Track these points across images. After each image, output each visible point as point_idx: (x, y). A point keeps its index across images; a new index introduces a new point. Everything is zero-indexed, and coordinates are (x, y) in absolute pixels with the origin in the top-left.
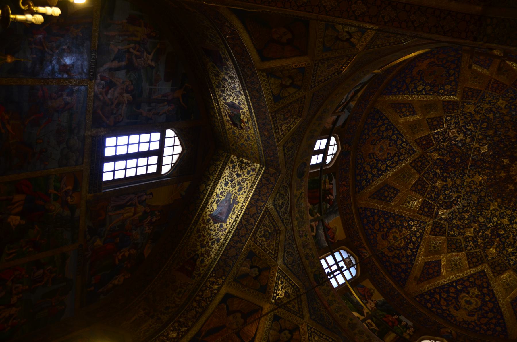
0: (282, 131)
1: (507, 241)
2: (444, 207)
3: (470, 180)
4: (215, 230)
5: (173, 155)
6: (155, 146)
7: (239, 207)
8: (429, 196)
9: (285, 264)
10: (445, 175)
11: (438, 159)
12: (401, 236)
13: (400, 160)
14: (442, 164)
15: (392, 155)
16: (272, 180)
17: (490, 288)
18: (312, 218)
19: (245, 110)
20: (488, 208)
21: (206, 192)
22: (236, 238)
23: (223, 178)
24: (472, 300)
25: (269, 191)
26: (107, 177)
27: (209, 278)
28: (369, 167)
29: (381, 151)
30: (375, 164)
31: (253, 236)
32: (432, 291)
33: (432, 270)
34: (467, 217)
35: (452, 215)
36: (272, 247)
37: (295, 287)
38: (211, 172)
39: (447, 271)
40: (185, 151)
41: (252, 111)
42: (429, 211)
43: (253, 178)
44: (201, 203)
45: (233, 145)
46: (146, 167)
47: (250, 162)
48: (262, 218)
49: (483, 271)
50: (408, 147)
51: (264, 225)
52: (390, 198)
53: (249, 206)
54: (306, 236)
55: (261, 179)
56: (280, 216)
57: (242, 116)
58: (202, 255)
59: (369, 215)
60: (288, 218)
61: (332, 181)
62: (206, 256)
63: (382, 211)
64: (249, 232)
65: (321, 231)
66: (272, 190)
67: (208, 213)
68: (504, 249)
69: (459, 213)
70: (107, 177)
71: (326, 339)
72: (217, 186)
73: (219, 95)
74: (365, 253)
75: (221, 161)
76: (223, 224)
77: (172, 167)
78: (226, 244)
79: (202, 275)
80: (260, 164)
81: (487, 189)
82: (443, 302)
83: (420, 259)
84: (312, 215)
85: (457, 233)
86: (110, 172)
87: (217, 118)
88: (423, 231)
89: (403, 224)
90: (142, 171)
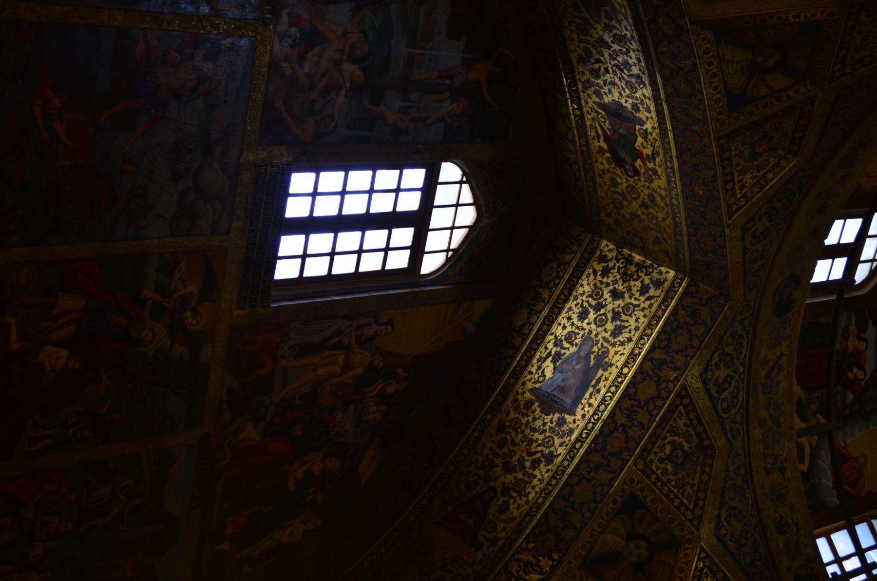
0: (742, 187)
4: (544, 431)
5: (452, 228)
6: (410, 202)
7: (612, 378)
9: (720, 538)
18: (803, 425)
19: (648, 126)
21: (530, 330)
23: (576, 298)
25: (695, 342)
26: (285, 270)
27: (517, 552)
31: (641, 456)
36: (688, 489)
38: (545, 279)
40: (485, 222)
41: (666, 130)
43: (655, 305)
44: (512, 358)
45: (609, 215)
46: (381, 252)
47: (649, 262)
51: (673, 432)
53: (638, 379)
54: (783, 470)
55: (675, 309)
56: (717, 412)
57: (640, 140)
58: (506, 491)
60: (739, 417)
61: (864, 331)
62: (514, 494)
64: (632, 444)
65: (825, 462)
66: (702, 341)
67: (530, 385)
70: (285, 270)
72: (560, 318)
73: (583, 83)
75: (575, 253)
76: (567, 417)
77: (448, 259)
78: (569, 471)
80: (677, 271)
84: (803, 418)
86: (296, 259)
87: (574, 141)
90: (371, 263)
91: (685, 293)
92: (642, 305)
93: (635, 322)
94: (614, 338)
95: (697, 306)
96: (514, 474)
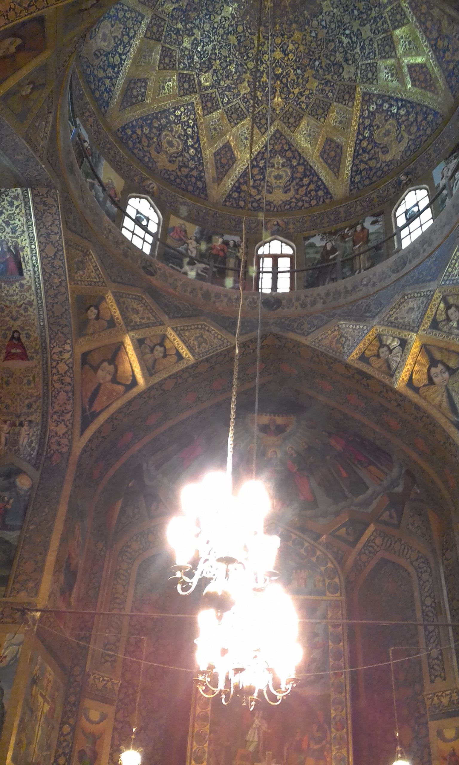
1: (289, 80)
2: (204, 70)
3: (220, 18)
4: (17, 294)
7: (29, 253)
8: (182, 66)
10: (189, 26)
11: (174, 9)
12: (174, 136)
13: (131, 38)
14: (180, 13)
15: (119, 37)
16: (50, 201)
17: (293, 149)
20: (252, 46)
22: (52, 292)
24: (281, 173)
28: (101, 71)
29: (105, 41)
30: (106, 62)
31: (70, 279)
32: (237, 185)
33: (225, 158)
34: (234, 70)
35: (217, 76)
36: (93, 275)
37: (137, 297)
39: (241, 152)
42: (190, 86)
48: (67, 253)
49: (277, 131)
50: (133, 15)
52: (142, 96)
53: (43, 247)
54: (110, 231)
59: (130, 133)
63: (140, 118)
64: (63, 278)
66: (59, 215)
68: (290, 93)
69: (224, 69)
71: (195, 328)
74: (151, 184)
76: (22, 282)
78: (44, 305)
79: (40, 351)
80: (21, 187)
81: (243, 20)
82: (253, 192)
83: (207, 153)
85: (232, 97)
88: (195, 115)
89: (169, 119)
91: (34, 196)
92: (16, 212)
93: (19, 221)
94: (15, 234)
95: (44, 199)
96: (20, 320)
